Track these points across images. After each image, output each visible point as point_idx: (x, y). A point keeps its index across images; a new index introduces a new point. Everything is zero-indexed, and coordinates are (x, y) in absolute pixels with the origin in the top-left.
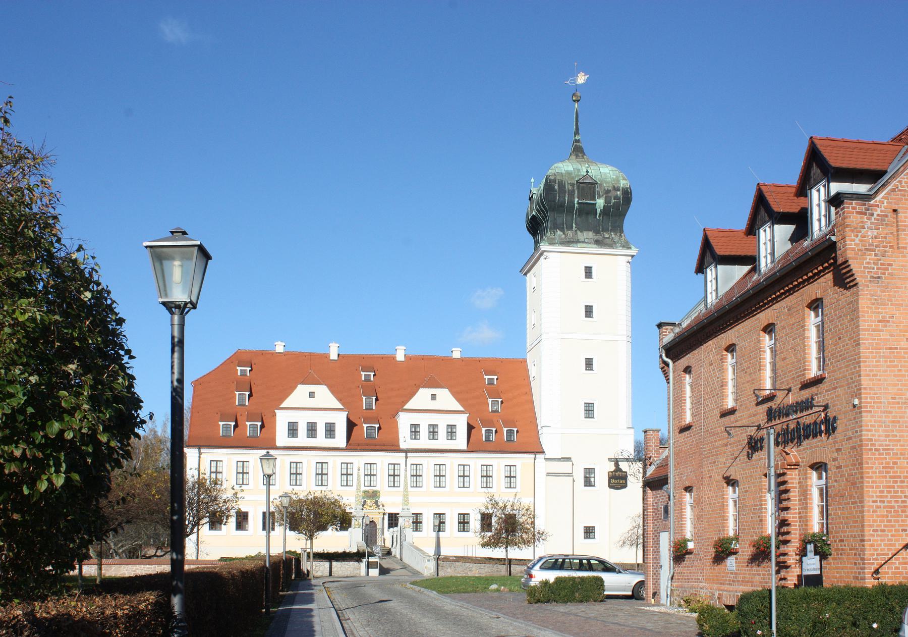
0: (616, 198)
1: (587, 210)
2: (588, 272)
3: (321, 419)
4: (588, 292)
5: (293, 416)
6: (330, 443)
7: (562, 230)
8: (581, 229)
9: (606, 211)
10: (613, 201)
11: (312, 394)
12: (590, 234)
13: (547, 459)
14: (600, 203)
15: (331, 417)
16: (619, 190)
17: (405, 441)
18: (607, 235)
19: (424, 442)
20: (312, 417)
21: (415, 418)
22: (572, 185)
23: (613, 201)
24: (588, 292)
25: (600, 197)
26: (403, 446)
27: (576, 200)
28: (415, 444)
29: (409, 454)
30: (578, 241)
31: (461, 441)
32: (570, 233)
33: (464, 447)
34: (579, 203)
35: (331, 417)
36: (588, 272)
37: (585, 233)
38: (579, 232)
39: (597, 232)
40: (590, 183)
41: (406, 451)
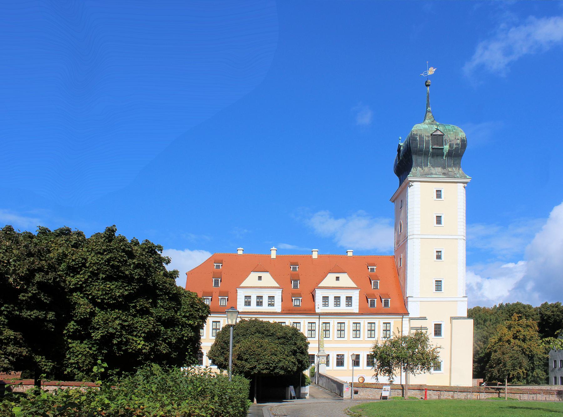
1: (438, 153)
2: (439, 194)
3: (266, 295)
4: (438, 207)
5: (248, 292)
6: (271, 309)
7: (421, 167)
8: (433, 166)
9: (450, 154)
10: (455, 146)
11: (260, 278)
12: (439, 169)
14: (446, 148)
15: (272, 293)
16: (458, 139)
17: (320, 308)
18: (450, 170)
19: (331, 308)
21: (326, 293)
22: (428, 137)
23: (455, 146)
24: (438, 207)
26: (317, 311)
30: (432, 174)
31: (355, 308)
32: (426, 169)
33: (357, 311)
34: (433, 149)
35: (272, 293)
36: (439, 194)
37: (436, 168)
38: (432, 168)
39: (444, 168)
40: (440, 135)
41: (320, 315)
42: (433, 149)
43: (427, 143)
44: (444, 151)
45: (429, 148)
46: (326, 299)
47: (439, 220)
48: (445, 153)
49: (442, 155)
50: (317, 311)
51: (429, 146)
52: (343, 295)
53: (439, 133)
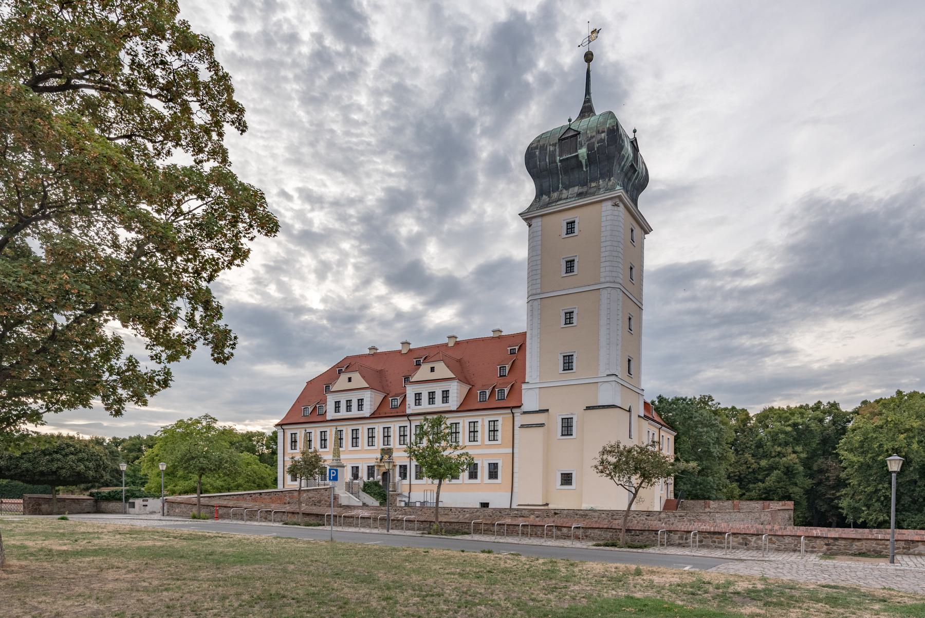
0: (602, 141)
3: (354, 397)
10: (596, 145)
13: (525, 413)
14: (583, 152)
16: (603, 132)
20: (349, 395)
22: (554, 145)
23: (596, 145)
25: (581, 147)
27: (558, 158)
28: (419, 409)
29: (411, 418)
39: (584, 183)
42: (561, 161)
43: (553, 155)
44: (581, 159)
45: (555, 162)
46: (337, 404)
47: (570, 265)
48: (584, 162)
49: (580, 164)
50: (408, 411)
51: (555, 158)
52: (438, 389)
53: (571, 133)
